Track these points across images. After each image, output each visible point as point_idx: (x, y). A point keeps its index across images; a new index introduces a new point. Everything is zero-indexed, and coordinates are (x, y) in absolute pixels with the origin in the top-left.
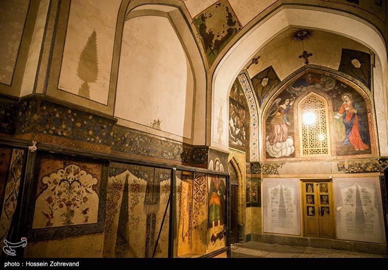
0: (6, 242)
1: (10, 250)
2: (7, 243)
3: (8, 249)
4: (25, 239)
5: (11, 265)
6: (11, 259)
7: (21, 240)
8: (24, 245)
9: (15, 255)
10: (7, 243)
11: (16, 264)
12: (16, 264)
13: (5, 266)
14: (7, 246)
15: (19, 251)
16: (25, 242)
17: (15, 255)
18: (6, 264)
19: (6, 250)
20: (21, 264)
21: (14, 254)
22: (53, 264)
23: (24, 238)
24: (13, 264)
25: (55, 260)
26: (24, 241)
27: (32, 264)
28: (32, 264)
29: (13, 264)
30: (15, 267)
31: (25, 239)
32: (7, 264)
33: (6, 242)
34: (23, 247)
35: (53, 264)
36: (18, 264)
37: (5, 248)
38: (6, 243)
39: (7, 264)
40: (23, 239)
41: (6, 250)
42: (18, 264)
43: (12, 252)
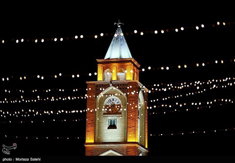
0: (4, 146)
1: (6, 151)
2: (5, 147)
3: (5, 150)
4: (15, 145)
5: (7, 160)
6: (7, 156)
7: (13, 145)
8: (15, 148)
9: (10, 154)
10: (5, 147)
11: (10, 159)
12: (10, 159)
13: (3, 160)
14: (6, 149)
15: (12, 151)
16: (15, 146)
17: (10, 154)
18: (4, 160)
19: (4, 151)
20: (13, 160)
21: (9, 153)
22: (32, 159)
23: (15, 144)
24: (8, 160)
25: (34, 158)
26: (15, 145)
27: (20, 160)
28: (20, 160)
29: (8, 160)
30: (9, 161)
31: (15, 145)
32: (4, 160)
33: (4, 146)
34: (14, 149)
35: (32, 159)
36: (11, 160)
37: (4, 150)
38: (4, 147)
39: (4, 160)
40: (14, 144)
41: (4, 151)
42: (11, 160)
43: (7, 152)
